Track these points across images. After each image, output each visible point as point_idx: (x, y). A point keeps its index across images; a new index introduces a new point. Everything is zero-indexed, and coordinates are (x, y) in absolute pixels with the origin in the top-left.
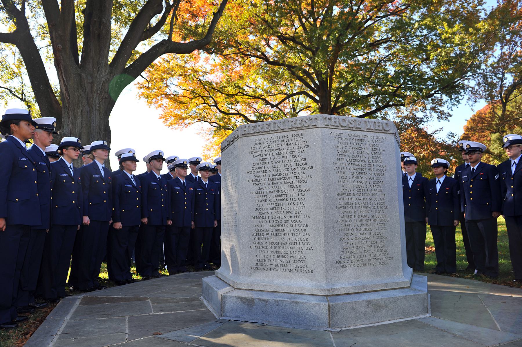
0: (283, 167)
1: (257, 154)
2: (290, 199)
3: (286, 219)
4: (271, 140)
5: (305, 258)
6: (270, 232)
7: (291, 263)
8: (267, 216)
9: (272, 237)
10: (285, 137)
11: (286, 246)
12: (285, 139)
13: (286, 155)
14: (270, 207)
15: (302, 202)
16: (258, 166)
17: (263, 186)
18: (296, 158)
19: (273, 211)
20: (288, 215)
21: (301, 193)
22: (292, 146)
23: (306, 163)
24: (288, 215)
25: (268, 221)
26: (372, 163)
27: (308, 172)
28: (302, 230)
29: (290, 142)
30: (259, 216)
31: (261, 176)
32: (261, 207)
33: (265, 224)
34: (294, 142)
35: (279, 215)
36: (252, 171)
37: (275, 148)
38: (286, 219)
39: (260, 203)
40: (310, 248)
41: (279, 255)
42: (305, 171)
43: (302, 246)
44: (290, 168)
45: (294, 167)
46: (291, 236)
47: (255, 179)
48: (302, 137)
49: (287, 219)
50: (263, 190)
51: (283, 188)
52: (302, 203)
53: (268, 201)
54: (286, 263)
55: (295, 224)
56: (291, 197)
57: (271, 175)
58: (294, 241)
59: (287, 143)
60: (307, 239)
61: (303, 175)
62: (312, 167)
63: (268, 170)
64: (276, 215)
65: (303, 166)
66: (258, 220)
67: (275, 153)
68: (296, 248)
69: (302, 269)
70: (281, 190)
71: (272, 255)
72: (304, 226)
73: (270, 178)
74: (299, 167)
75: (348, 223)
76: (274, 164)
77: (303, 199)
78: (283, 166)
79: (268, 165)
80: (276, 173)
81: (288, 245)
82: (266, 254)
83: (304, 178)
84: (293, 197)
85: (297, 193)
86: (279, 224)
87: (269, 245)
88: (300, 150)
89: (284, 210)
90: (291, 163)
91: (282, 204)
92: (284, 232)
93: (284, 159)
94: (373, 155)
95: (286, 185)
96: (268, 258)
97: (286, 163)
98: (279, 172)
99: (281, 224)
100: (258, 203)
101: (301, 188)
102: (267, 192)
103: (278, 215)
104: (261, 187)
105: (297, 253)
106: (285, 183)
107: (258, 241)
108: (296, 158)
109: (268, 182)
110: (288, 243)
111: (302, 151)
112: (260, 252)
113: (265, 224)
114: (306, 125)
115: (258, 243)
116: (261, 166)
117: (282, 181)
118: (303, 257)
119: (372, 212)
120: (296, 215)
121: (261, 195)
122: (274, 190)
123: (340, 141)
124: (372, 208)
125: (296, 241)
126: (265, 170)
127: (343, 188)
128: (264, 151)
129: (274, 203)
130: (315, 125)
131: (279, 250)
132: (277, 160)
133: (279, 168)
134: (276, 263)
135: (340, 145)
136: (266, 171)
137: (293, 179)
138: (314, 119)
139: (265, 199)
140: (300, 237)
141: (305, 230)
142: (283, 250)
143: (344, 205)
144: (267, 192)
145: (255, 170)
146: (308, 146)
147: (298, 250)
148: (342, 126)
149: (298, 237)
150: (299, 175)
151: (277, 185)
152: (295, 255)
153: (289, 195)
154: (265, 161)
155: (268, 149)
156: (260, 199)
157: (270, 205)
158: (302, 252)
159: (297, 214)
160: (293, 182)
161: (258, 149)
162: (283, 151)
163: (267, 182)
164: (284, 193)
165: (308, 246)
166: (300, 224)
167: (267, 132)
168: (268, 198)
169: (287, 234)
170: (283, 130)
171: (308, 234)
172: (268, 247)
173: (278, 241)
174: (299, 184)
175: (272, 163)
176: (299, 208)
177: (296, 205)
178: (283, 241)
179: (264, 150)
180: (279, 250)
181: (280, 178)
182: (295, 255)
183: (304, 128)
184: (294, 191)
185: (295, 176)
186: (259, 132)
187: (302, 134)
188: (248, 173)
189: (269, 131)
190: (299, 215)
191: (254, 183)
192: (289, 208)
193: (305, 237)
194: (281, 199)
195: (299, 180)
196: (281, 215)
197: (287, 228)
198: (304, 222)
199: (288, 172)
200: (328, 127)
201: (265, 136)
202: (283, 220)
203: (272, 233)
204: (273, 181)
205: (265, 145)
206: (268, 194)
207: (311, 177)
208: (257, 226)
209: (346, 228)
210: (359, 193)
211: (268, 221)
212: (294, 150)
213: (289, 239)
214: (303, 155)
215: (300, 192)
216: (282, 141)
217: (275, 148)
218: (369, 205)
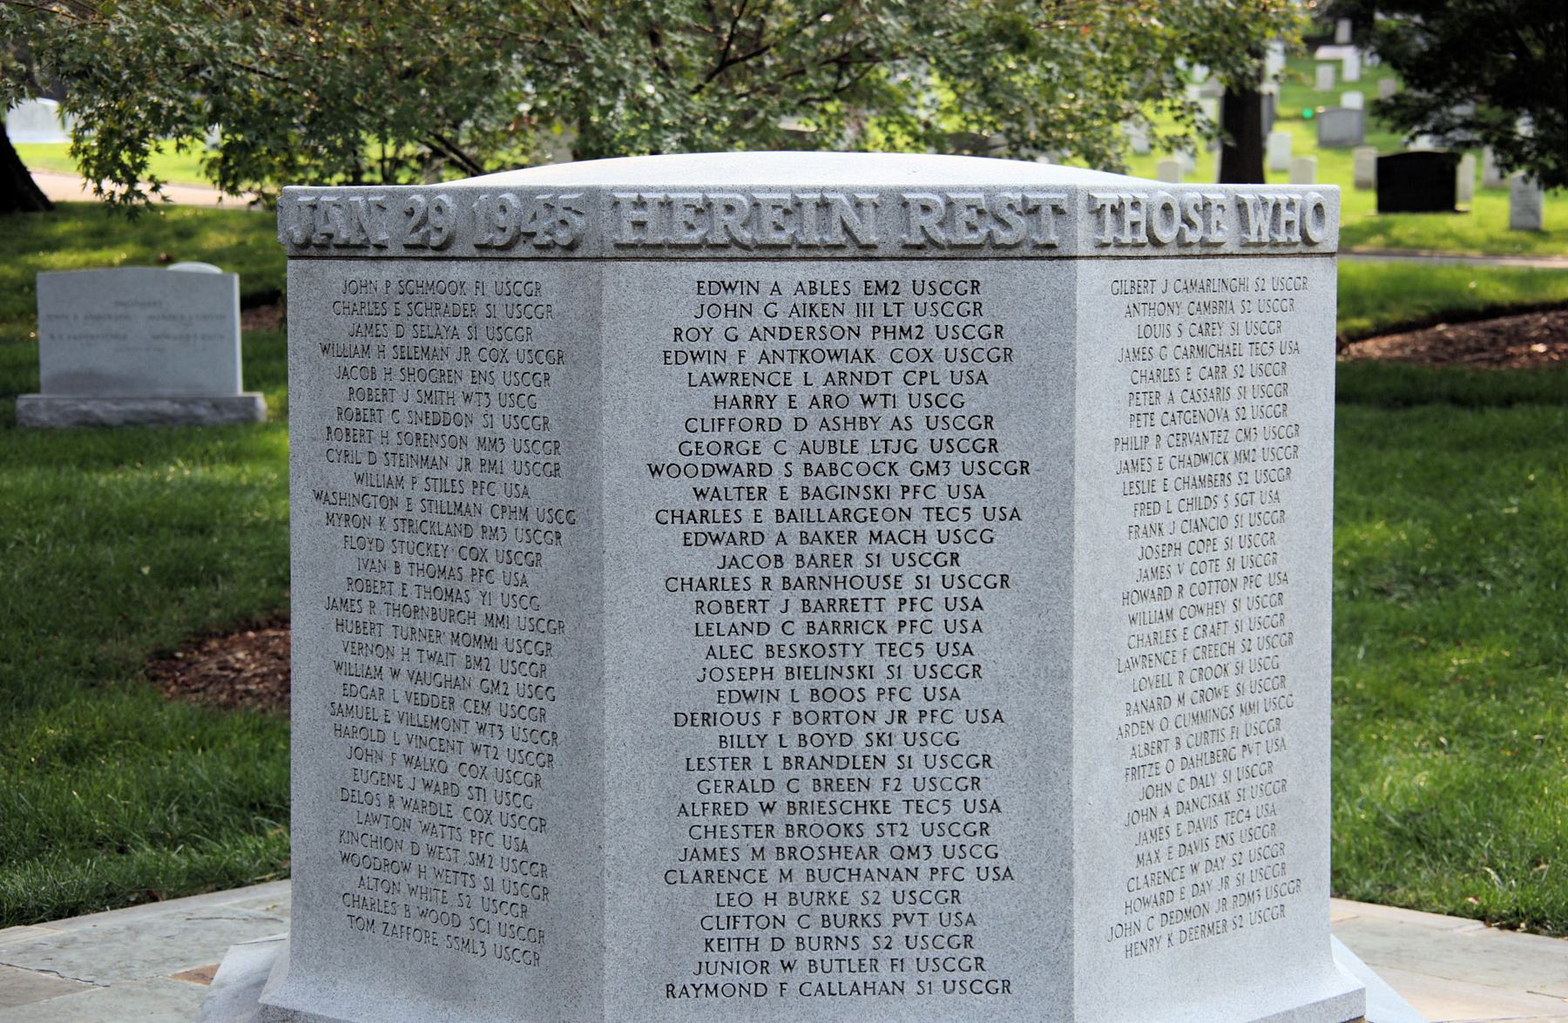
0: (864, 454)
1: (709, 369)
2: (902, 624)
3: (872, 728)
4: (800, 299)
5: (971, 920)
6: (781, 797)
7: (899, 951)
8: (766, 710)
9: (794, 820)
10: (882, 287)
11: (873, 864)
12: (879, 300)
13: (881, 388)
14: (787, 662)
15: (963, 640)
16: (716, 436)
17: (745, 549)
18: (941, 413)
19: (803, 687)
20: (885, 708)
21: (960, 593)
22: (919, 344)
23: (993, 444)
24: (885, 708)
25: (773, 739)
26: (1250, 423)
27: (1001, 490)
28: (961, 784)
29: (911, 319)
30: (720, 709)
31: (733, 493)
32: (729, 663)
33: (756, 755)
34: (929, 323)
35: (839, 705)
36: (682, 461)
37: (818, 344)
38: (872, 728)
39: (725, 642)
40: (1001, 872)
41: (830, 910)
42: (986, 481)
43: (956, 862)
44: (904, 460)
45: (926, 455)
46: (898, 813)
47: (697, 505)
48: (976, 297)
49: (880, 725)
50: (743, 573)
51: (859, 567)
52: (962, 647)
53: (776, 628)
54: (872, 954)
55: (923, 751)
56: (906, 615)
57: (793, 493)
58: (915, 838)
59: (889, 322)
60: (984, 828)
61: (976, 505)
62: (1025, 467)
63: (778, 464)
64: (820, 706)
65: (977, 457)
66: (711, 733)
67: (818, 371)
68: (924, 873)
69: (958, 976)
70: (850, 572)
71: (791, 914)
72: (973, 761)
73: (786, 507)
74: (956, 458)
76: (813, 434)
77: (970, 625)
78: (864, 448)
79: (775, 436)
80: (823, 482)
81: (884, 861)
82: (759, 908)
83: (977, 521)
84: (919, 615)
85: (937, 591)
86: (837, 750)
87: (773, 865)
88: (965, 367)
89: (862, 683)
90: (911, 434)
91: (851, 650)
92: (864, 796)
93: (868, 412)
94: (1258, 381)
95: (876, 548)
96: (770, 932)
97: (884, 431)
98: (839, 480)
99: (849, 751)
100: (717, 641)
101: (965, 568)
102: (766, 582)
103: (831, 707)
104: (732, 550)
105: (927, 897)
106: (875, 537)
107: (712, 843)
108: (941, 413)
109: (778, 528)
110: (884, 850)
111: (976, 375)
112: (723, 900)
113: (756, 755)
114: (1004, 237)
116: (735, 436)
117: (855, 526)
118: (964, 917)
119: (1239, 669)
120: (928, 707)
121: (734, 597)
122: (809, 571)
124: (1239, 648)
125: (925, 840)
126: (756, 459)
127: (1145, 564)
128: (752, 358)
129: (811, 640)
130: (1051, 246)
131: (832, 886)
132: (829, 413)
133: (840, 459)
134: (817, 956)
135: (1139, 343)
136: (765, 470)
137: (918, 522)
138: (1046, 210)
139: (755, 618)
140: (948, 819)
141: (975, 781)
142: (856, 888)
143: (1144, 651)
144: (766, 582)
145: (699, 461)
146: (1008, 354)
147: (938, 883)
148: (1156, 243)
149: (938, 818)
150: (950, 503)
151: (829, 550)
152: (920, 907)
153: (891, 606)
154: (759, 413)
155: (780, 345)
156: (725, 619)
157: (787, 652)
158: (955, 895)
159: (936, 704)
160: (919, 536)
161: (717, 342)
162: (865, 367)
163: (769, 525)
164: (866, 592)
165: (991, 863)
166: (951, 751)
167: (775, 252)
168: (774, 616)
169: (880, 806)
170: (867, 253)
171: (989, 803)
172: (772, 875)
173: (826, 840)
174: (951, 547)
175: (800, 424)
176: (950, 671)
177: (931, 658)
178: (854, 843)
179: (754, 349)
180: (832, 886)
181: (846, 513)
182: (920, 907)
183: (991, 253)
184: (923, 583)
185: (933, 504)
186: (725, 246)
187: (975, 285)
188: (655, 471)
189: (788, 247)
190: (946, 705)
191: (691, 527)
192: (894, 672)
193: (977, 817)
194: (848, 625)
195: (951, 526)
196: (845, 707)
197: (877, 775)
198: (974, 739)
199: (895, 483)
200: (1105, 252)
201: (764, 272)
202: (859, 731)
203: (795, 798)
204: (805, 526)
205: (759, 321)
206: (777, 595)
207: (1015, 514)
208: (706, 763)
210: (1199, 578)
211: (773, 739)
212: (927, 367)
213: (887, 829)
214: (977, 400)
215: (955, 592)
216: (863, 310)
217: (818, 344)
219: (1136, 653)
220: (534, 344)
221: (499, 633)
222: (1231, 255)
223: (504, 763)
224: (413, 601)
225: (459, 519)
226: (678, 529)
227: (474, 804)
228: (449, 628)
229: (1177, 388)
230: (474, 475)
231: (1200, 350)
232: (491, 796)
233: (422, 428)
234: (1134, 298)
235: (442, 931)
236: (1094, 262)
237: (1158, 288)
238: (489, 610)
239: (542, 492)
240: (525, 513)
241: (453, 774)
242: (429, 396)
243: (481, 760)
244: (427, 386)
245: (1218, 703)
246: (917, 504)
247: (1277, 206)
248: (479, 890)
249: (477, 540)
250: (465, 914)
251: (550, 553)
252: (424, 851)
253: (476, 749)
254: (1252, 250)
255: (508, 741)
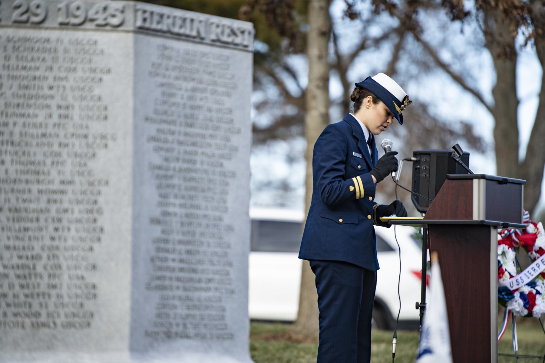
8: (174, 219)
24: (204, 222)
29: (211, 69)
36: (154, 116)
51: (198, 166)
115: (159, 278)
220: (93, 66)
221: (69, 188)
223: (70, 242)
224: (13, 176)
225: (44, 140)
226: (152, 144)
227: (51, 262)
228: (35, 188)
230: (55, 119)
232: (61, 258)
233: (21, 101)
235: (28, 321)
238: (62, 178)
239: (96, 127)
240: (86, 136)
241: (37, 250)
242: (27, 87)
243: (56, 243)
244: (25, 82)
246: (213, 142)
248: (54, 299)
249: (56, 148)
250: (44, 312)
251: (101, 153)
252: (17, 288)
253: (53, 239)
255: (73, 232)
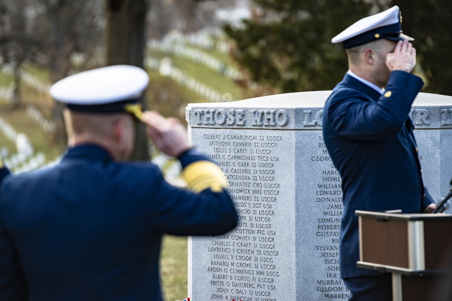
75: (223, 273)
94: (262, 169)
123: (216, 147)
124: (256, 253)
200: (201, 126)
209: (220, 280)
218: (252, 248)
219: (215, 246)
222: (249, 129)
229: (230, 168)
231: (238, 157)
234: (212, 140)
236: (197, 129)
237: (221, 138)
245: (248, 268)
247: (263, 114)
254: (259, 127)
